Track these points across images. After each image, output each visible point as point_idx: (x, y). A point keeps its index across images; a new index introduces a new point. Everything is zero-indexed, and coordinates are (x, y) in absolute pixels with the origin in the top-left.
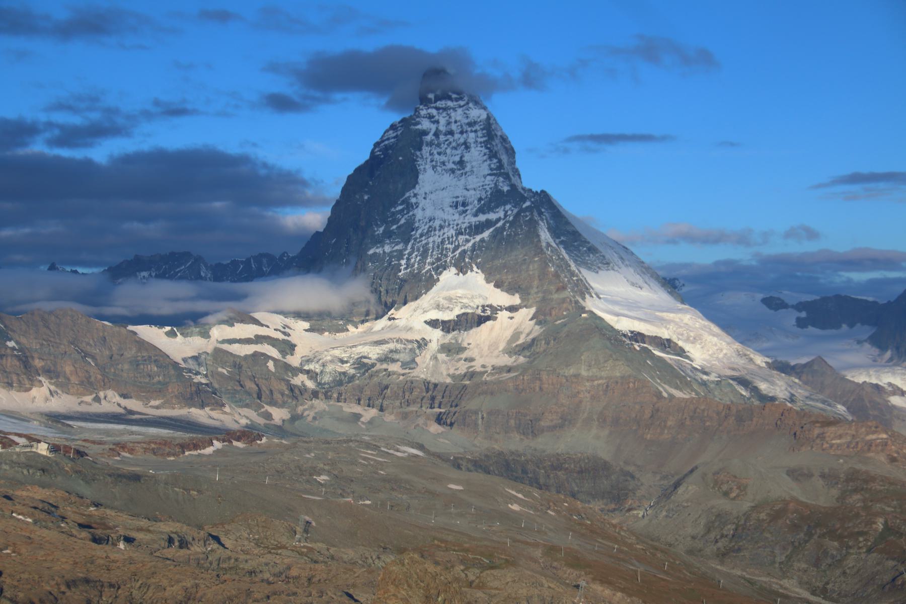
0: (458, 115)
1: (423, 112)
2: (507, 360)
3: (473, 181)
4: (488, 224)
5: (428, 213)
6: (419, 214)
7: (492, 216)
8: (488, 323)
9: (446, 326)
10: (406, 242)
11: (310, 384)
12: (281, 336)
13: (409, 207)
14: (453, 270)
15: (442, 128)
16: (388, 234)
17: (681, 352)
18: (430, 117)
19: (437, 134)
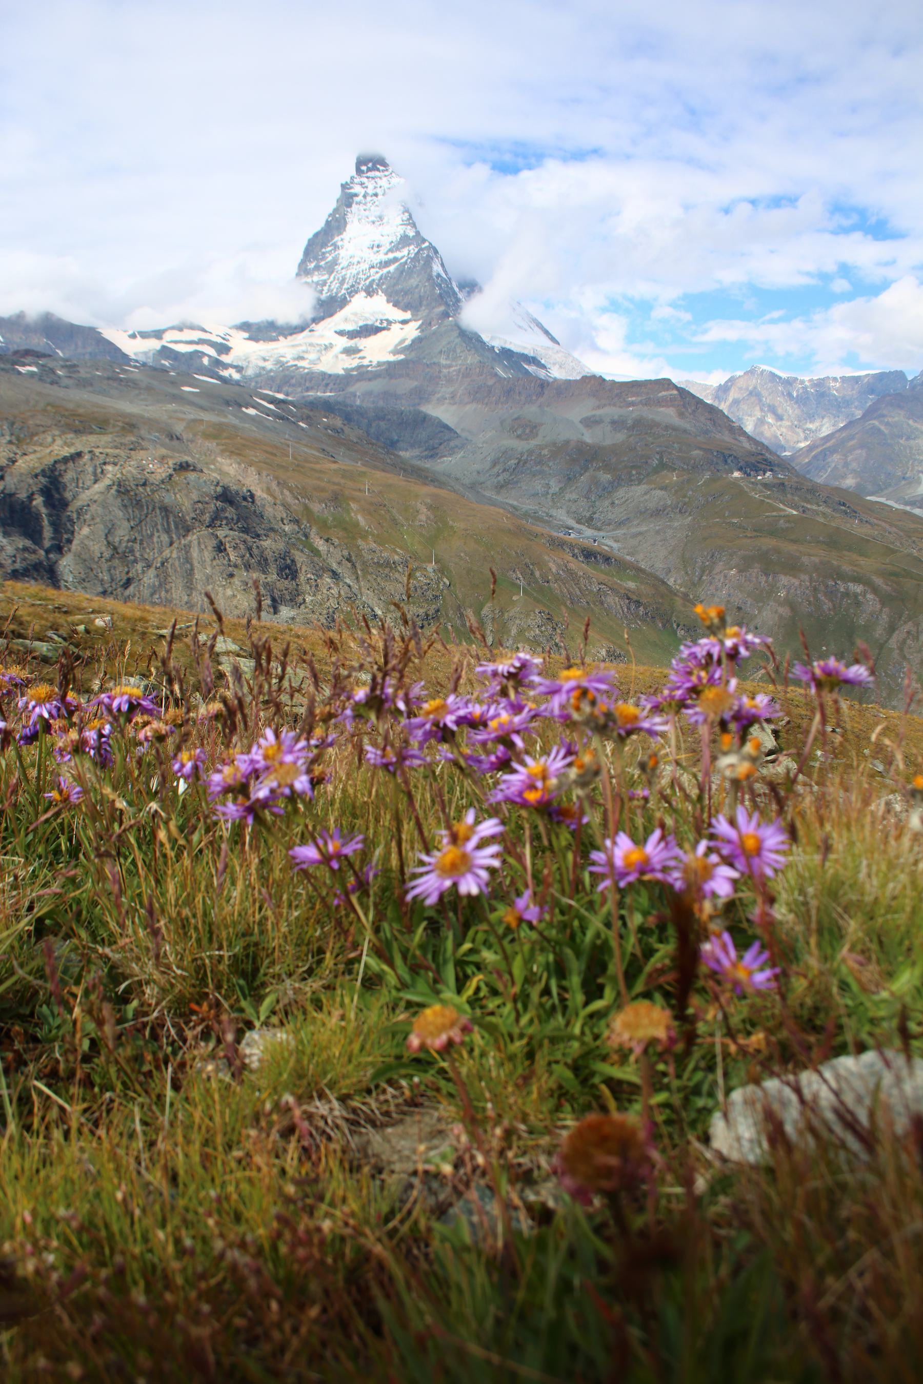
0: (383, 182)
1: (357, 180)
2: (392, 358)
4: (395, 260)
6: (342, 253)
7: (398, 254)
8: (384, 333)
9: (352, 335)
10: (330, 273)
11: (236, 376)
12: (219, 340)
13: (336, 247)
14: (363, 294)
16: (317, 268)
17: (543, 367)
18: (362, 184)
19: (365, 196)
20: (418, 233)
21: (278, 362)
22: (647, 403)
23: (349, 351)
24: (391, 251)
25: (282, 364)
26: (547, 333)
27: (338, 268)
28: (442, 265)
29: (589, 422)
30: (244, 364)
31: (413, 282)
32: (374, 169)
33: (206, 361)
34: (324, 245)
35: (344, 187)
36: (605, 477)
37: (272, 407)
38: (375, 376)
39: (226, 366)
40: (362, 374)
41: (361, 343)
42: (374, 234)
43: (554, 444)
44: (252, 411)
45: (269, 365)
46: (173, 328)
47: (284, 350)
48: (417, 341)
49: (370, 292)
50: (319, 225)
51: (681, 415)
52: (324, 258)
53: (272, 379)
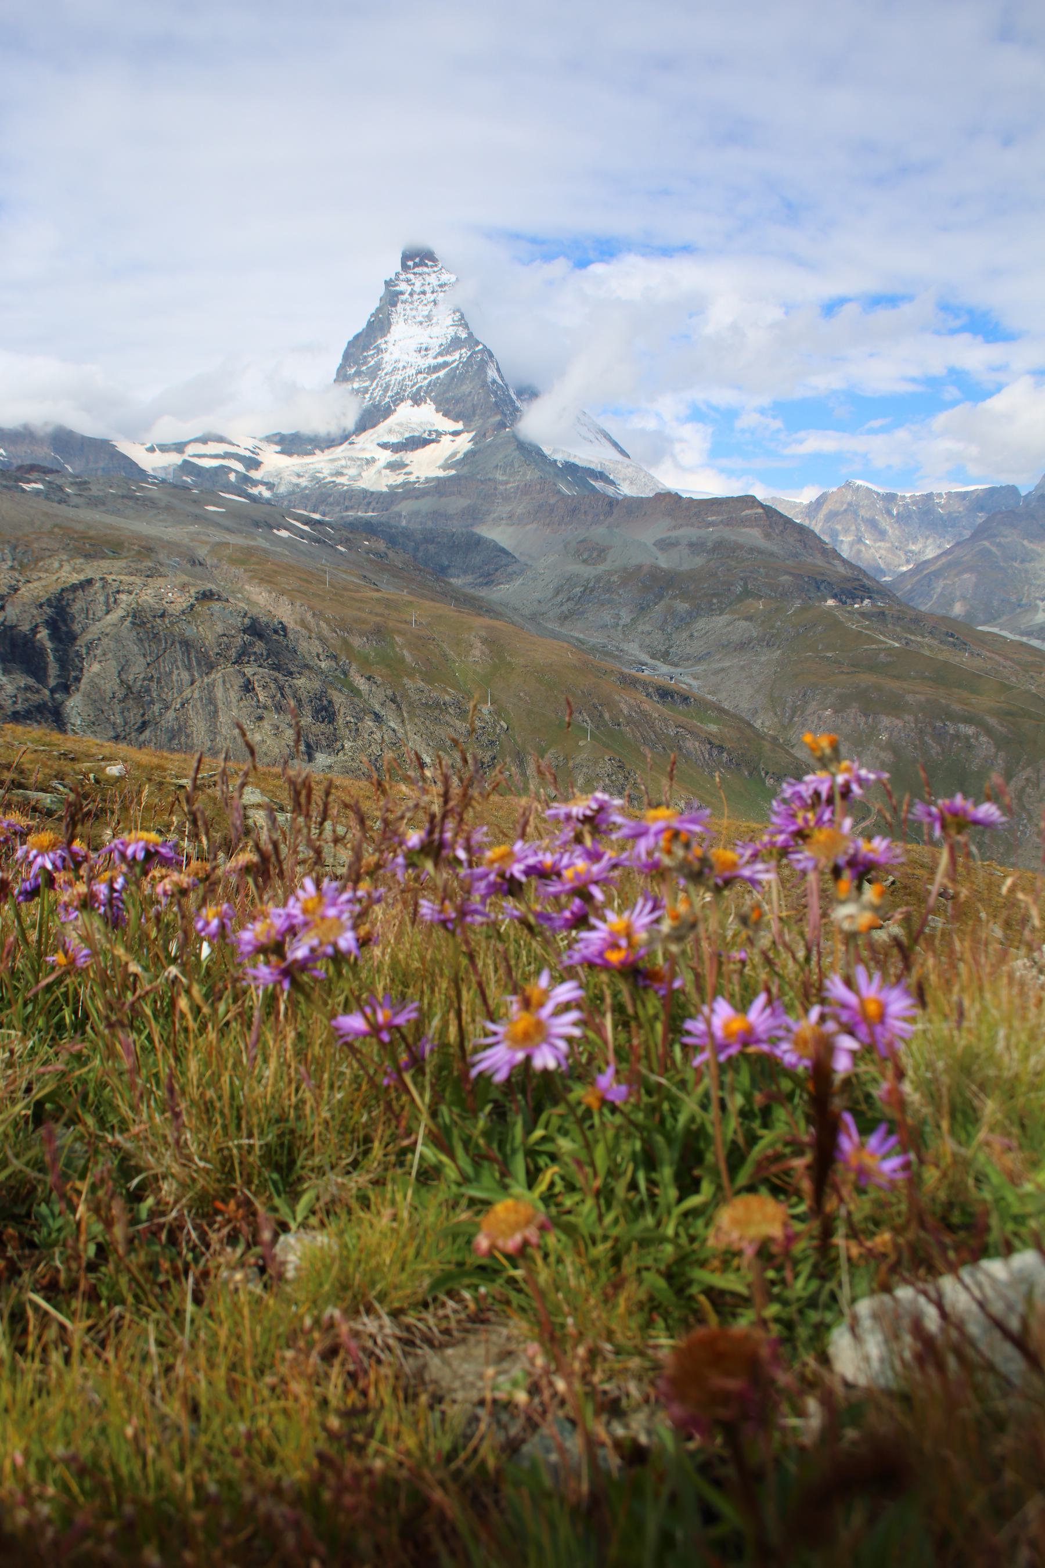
0: (433, 279)
2: (441, 474)
3: (436, 331)
4: (446, 364)
5: (395, 357)
6: (386, 357)
7: (448, 358)
9: (397, 448)
11: (267, 494)
12: (248, 454)
13: (379, 351)
14: (410, 402)
15: (417, 289)
16: (358, 373)
18: (408, 281)
20: (470, 335)
21: (314, 478)
22: (729, 523)
23: (393, 466)
24: (440, 354)
25: (319, 481)
26: (615, 445)
27: (382, 374)
28: (498, 370)
29: (664, 545)
30: (276, 481)
31: (466, 388)
32: (422, 264)
33: (232, 477)
34: (366, 348)
35: (388, 284)
36: (682, 606)
37: (306, 528)
38: (423, 493)
39: (255, 483)
40: (409, 491)
41: (408, 457)
42: (422, 336)
43: (625, 569)
44: (284, 534)
45: (304, 482)
46: (196, 440)
47: (321, 464)
48: (470, 455)
49: (417, 400)
50: (361, 326)
51: (767, 536)
52: (365, 363)
53: (307, 497)
